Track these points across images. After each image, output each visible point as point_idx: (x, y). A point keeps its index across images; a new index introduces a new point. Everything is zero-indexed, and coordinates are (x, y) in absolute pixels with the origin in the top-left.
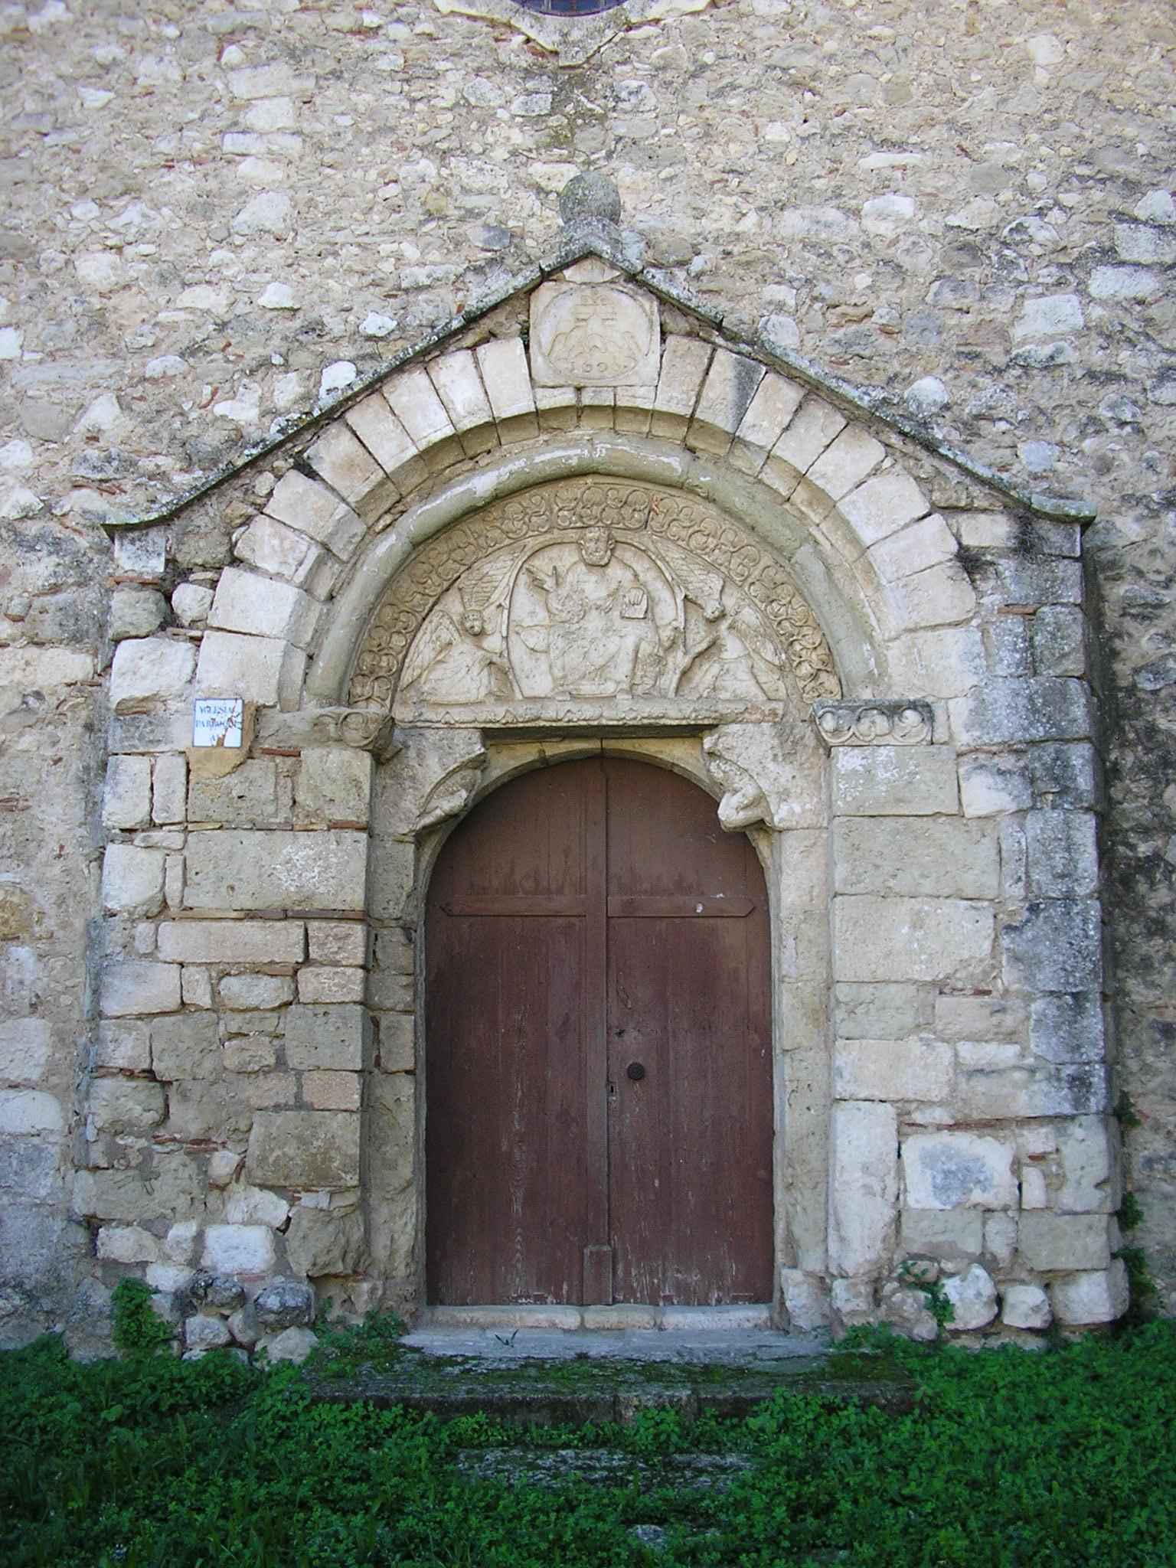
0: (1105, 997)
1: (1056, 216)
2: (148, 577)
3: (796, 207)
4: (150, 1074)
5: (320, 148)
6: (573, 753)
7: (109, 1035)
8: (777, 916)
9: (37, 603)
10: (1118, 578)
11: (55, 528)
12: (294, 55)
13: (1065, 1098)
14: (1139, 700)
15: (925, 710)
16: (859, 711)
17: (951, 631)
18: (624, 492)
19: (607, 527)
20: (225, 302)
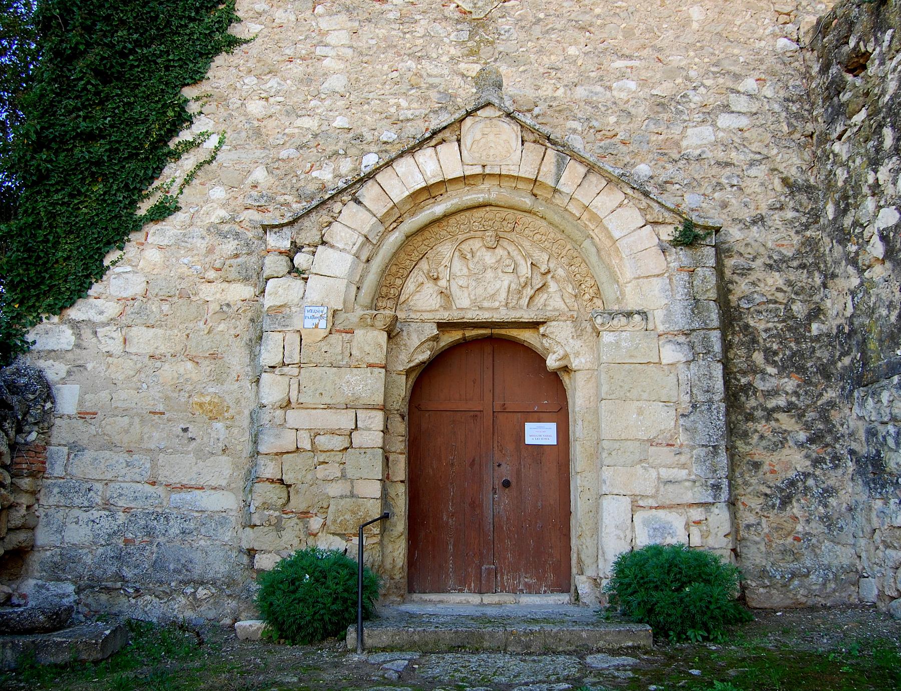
0: (727, 449)
1: (702, 90)
2: (283, 250)
3: (582, 85)
4: (281, 481)
5: (361, 54)
6: (478, 335)
7: (262, 463)
8: (574, 411)
9: (228, 262)
10: (731, 256)
11: (237, 228)
13: (709, 495)
14: (741, 312)
15: (644, 314)
16: (612, 315)
17: (655, 279)
18: (503, 215)
19: (496, 230)
20: (317, 125)
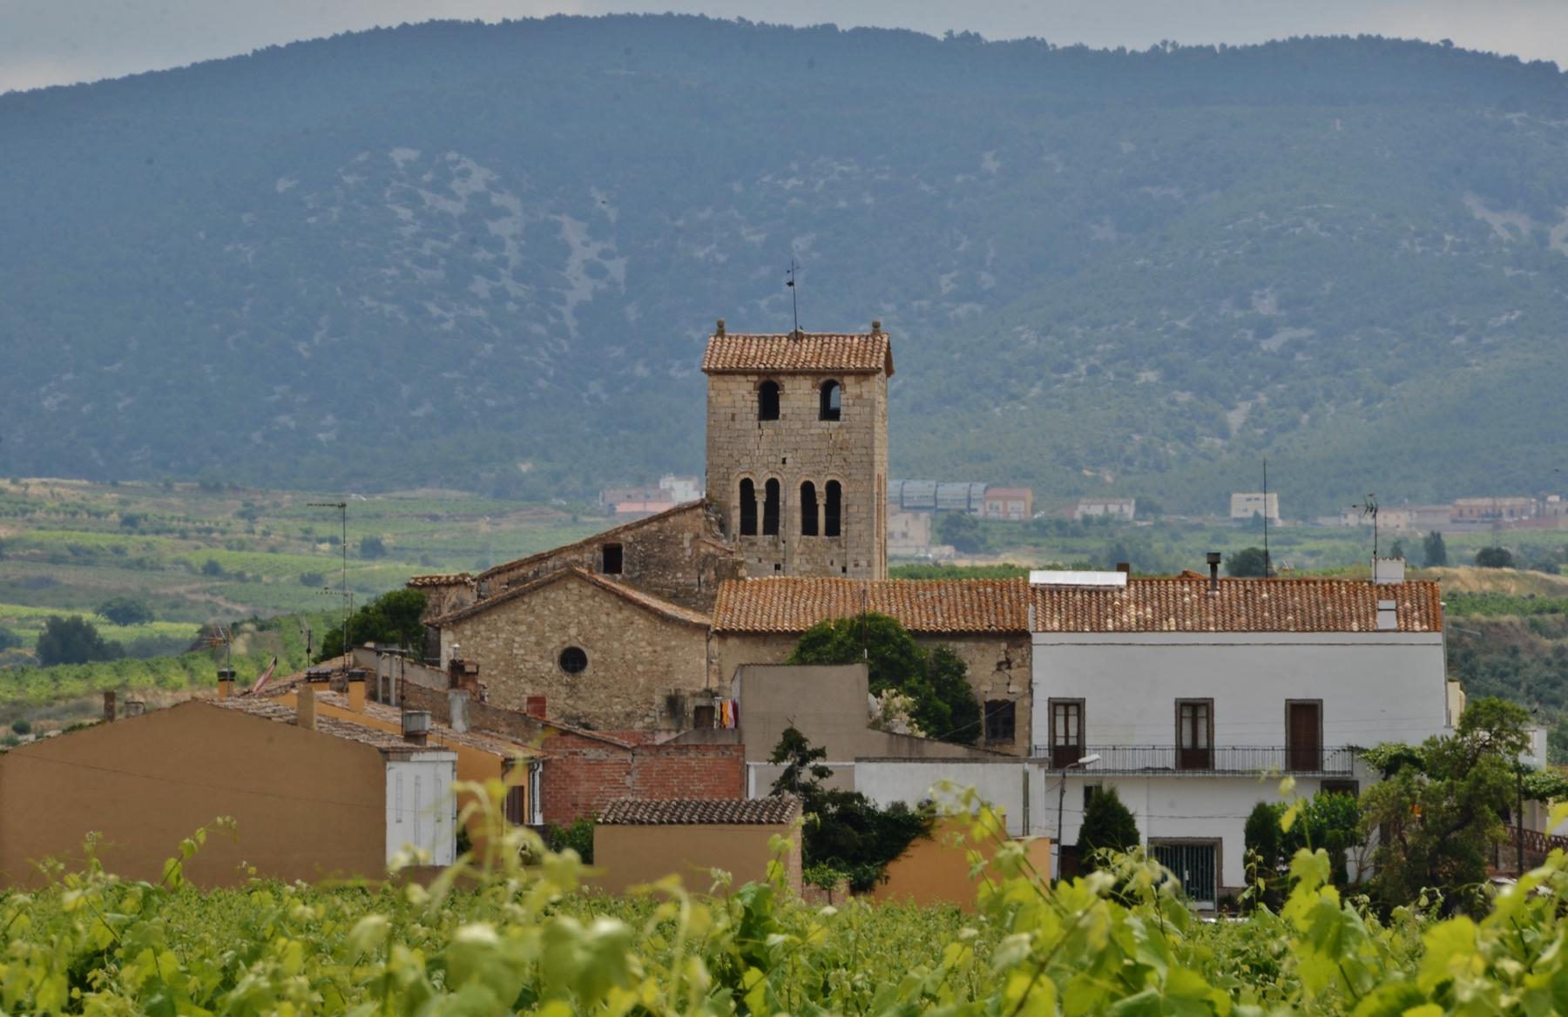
12: (532, 681)
